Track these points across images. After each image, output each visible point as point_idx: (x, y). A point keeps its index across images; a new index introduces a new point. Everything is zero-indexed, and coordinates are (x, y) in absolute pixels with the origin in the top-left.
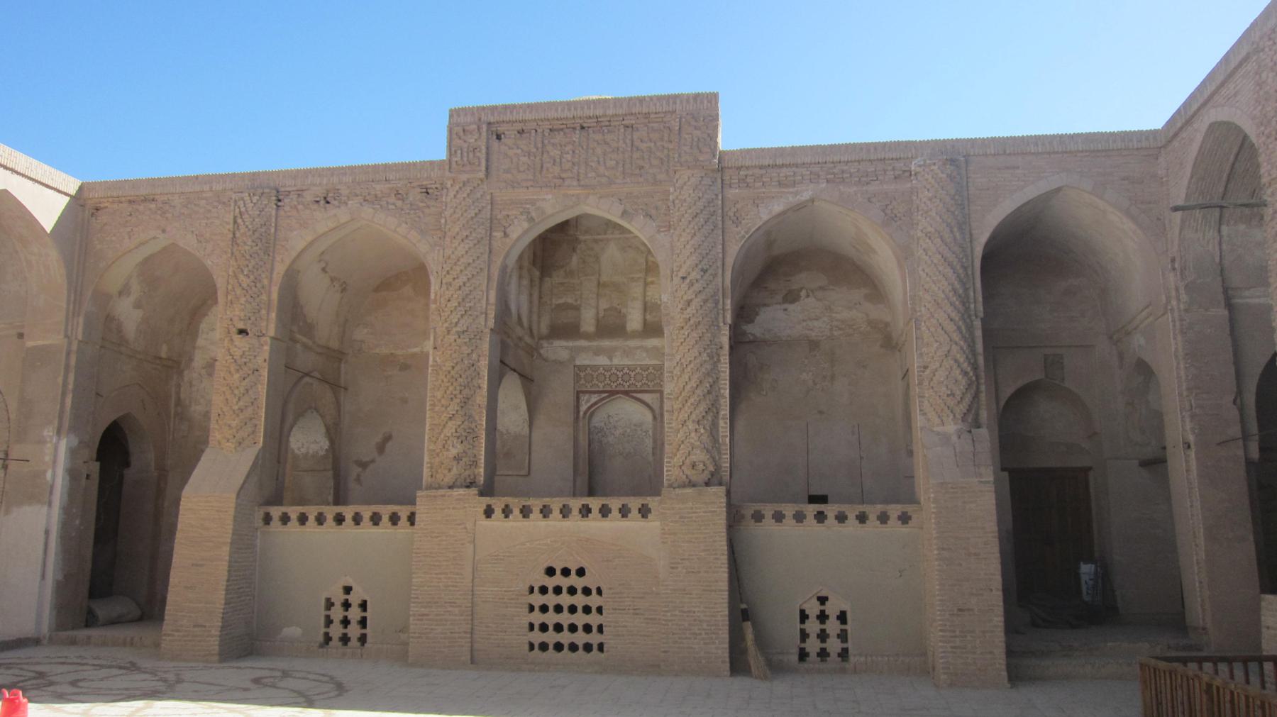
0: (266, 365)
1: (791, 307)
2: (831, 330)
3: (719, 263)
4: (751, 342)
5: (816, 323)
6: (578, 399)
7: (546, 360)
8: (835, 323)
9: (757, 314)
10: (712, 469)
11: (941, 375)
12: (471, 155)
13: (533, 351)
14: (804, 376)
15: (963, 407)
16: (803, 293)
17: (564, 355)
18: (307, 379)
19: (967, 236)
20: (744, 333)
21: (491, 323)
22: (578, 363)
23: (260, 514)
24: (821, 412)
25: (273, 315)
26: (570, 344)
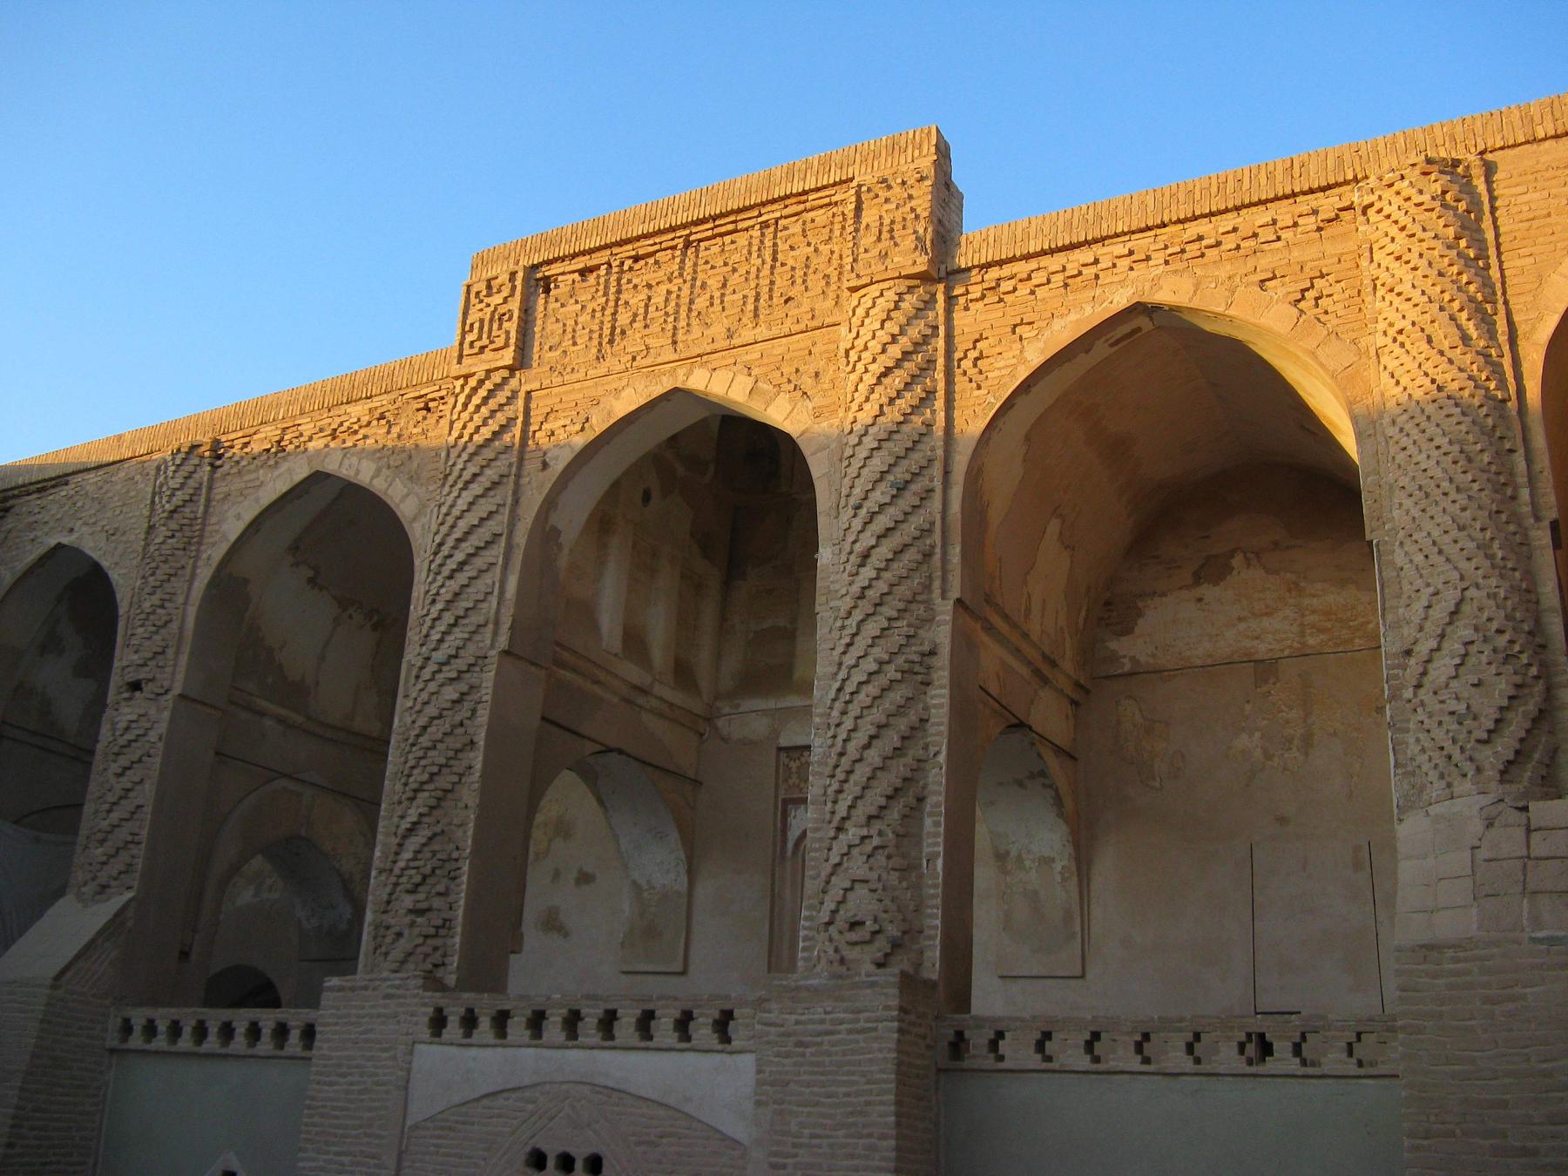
0: (160, 745)
1: (1208, 591)
2: (1302, 634)
3: (937, 470)
4: (1131, 674)
5: (1266, 622)
6: (785, 815)
7: (725, 740)
8: (1311, 619)
9: (1140, 614)
10: (893, 930)
11: (1442, 668)
12: (495, 326)
13: (701, 724)
14: (1242, 741)
15: (1505, 746)
16: (1237, 561)
17: (759, 727)
18: (284, 783)
19: (1501, 326)
20: (1114, 658)
21: (503, 641)
22: (783, 742)
23: (114, 1023)
24: (1282, 820)
25: (184, 659)
26: (771, 704)
